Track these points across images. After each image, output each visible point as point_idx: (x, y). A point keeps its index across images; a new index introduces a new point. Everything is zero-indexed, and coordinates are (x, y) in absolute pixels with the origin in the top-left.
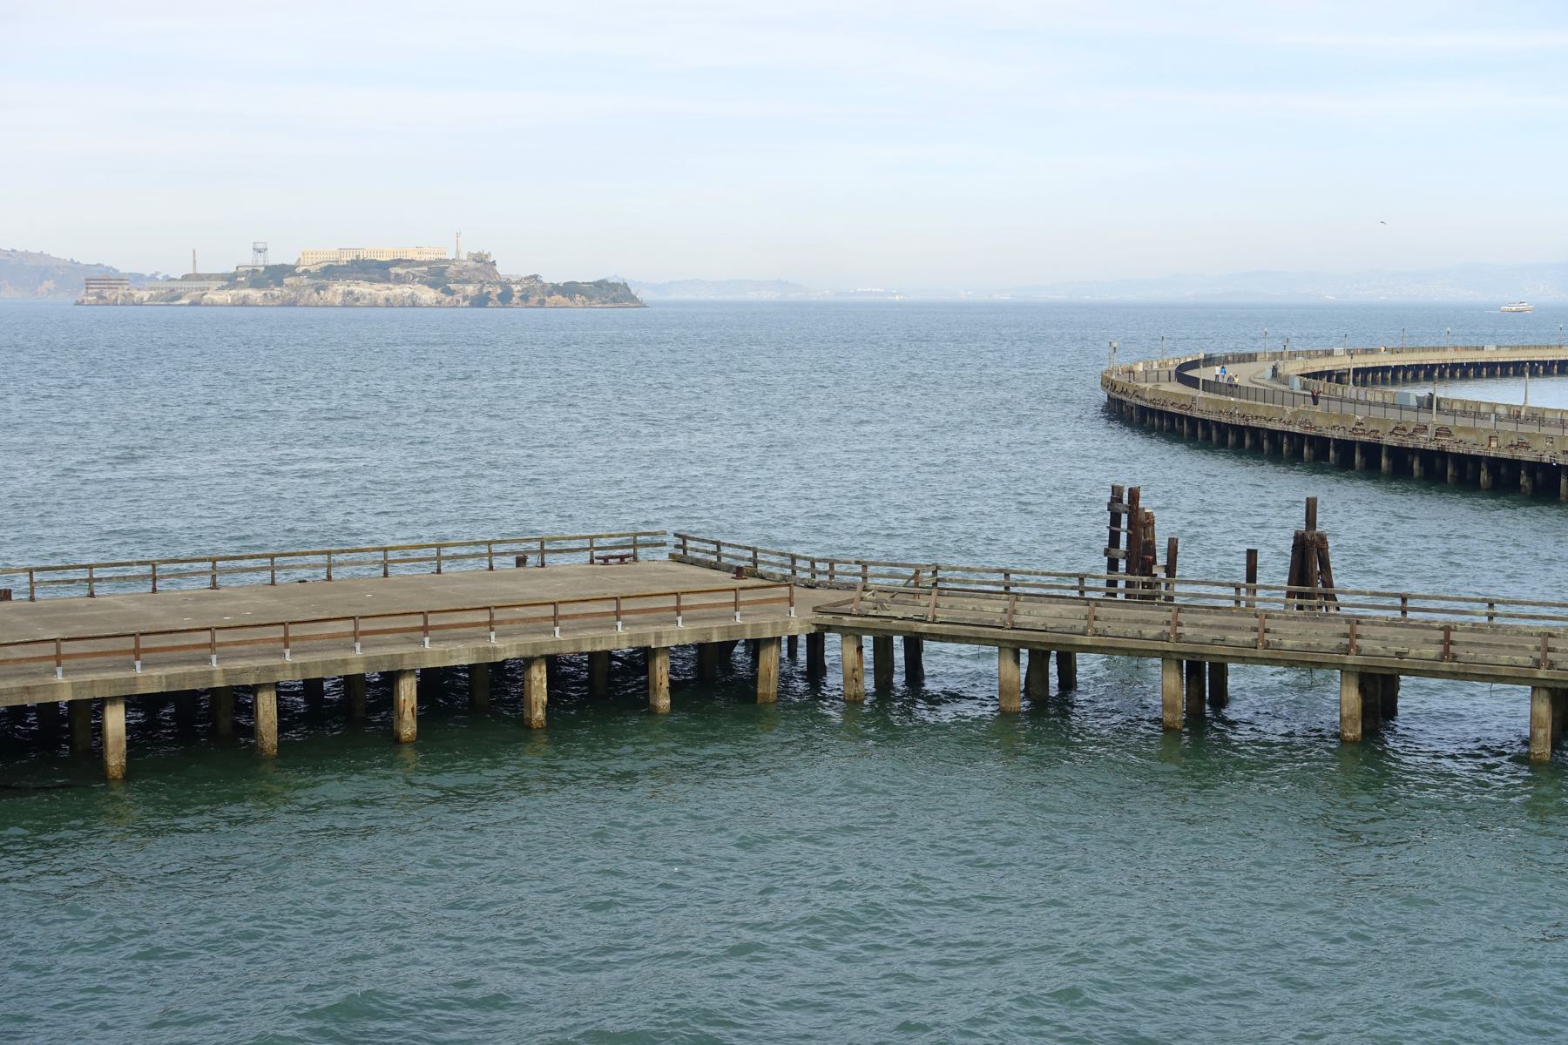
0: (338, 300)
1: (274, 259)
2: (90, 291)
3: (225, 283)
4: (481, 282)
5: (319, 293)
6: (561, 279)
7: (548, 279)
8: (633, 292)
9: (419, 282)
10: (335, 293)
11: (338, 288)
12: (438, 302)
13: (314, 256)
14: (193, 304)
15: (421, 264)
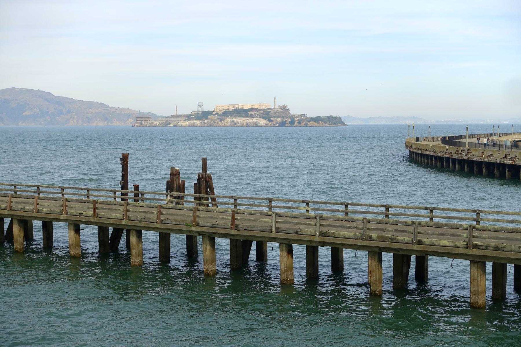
0: (229, 124)
1: (205, 109)
2: (137, 122)
3: (187, 118)
4: (283, 117)
5: (221, 122)
6: (313, 115)
7: (309, 115)
8: (342, 120)
9: (259, 117)
10: (227, 121)
11: (228, 120)
12: (266, 125)
13: (220, 107)
14: (175, 126)
15: (261, 110)
